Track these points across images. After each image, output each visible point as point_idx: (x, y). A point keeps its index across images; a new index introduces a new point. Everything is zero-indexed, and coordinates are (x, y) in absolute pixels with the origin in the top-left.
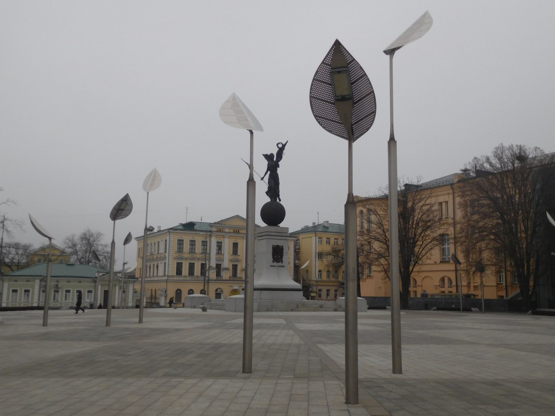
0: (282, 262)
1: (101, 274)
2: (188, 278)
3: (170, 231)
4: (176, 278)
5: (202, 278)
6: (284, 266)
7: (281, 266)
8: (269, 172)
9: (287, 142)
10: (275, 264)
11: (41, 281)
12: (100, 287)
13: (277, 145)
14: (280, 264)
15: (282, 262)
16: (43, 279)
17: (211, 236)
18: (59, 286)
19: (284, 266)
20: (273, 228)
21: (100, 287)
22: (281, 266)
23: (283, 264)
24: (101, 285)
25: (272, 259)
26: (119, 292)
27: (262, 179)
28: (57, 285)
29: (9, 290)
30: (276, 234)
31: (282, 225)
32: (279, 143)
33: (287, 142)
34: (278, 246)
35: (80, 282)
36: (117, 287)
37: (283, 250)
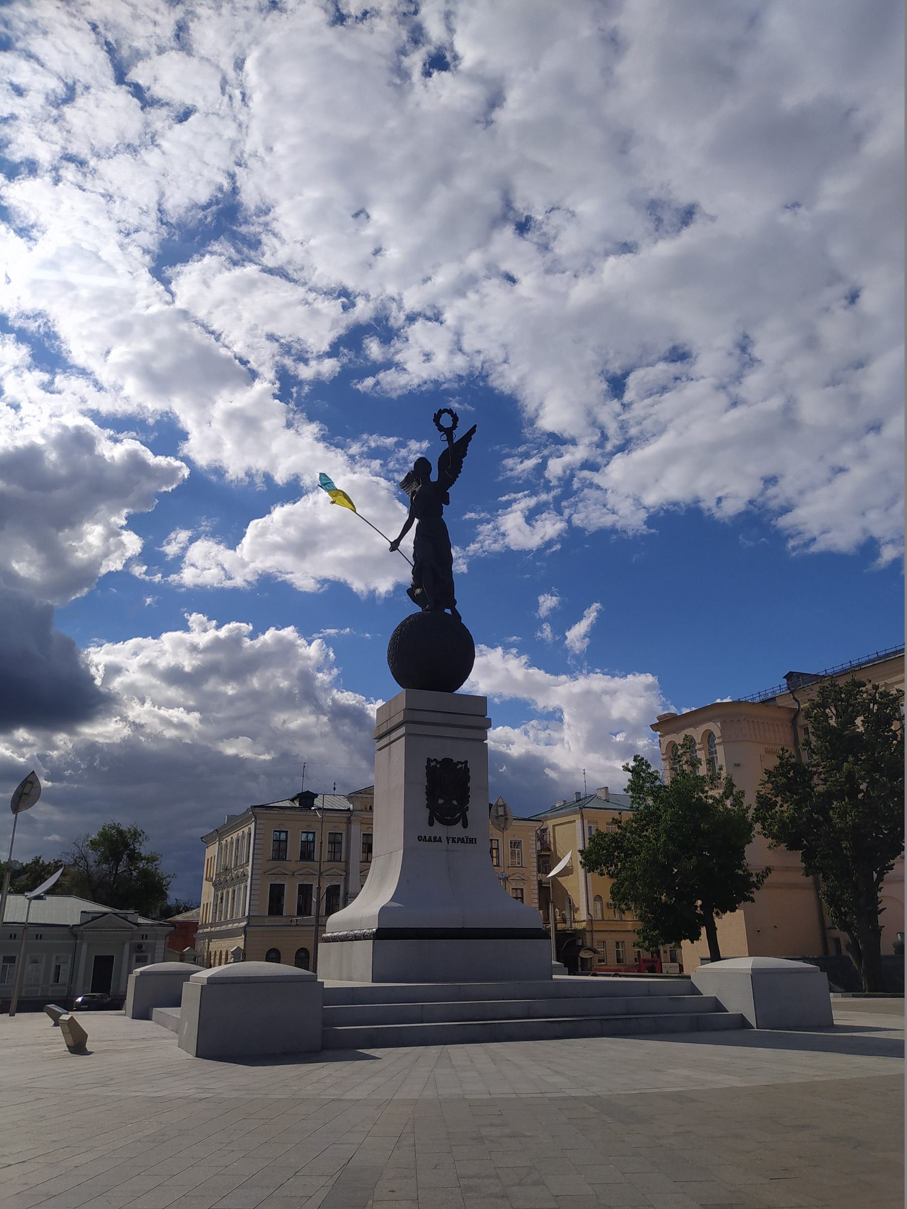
0: (465, 825)
3: (257, 810)
6: (472, 841)
7: (462, 840)
8: (416, 521)
10: (438, 829)
12: (84, 947)
13: (437, 419)
14: (457, 830)
15: (465, 825)
17: (349, 822)
19: (472, 841)
21: (84, 947)
22: (462, 840)
23: (469, 833)
25: (426, 812)
27: (395, 545)
30: (439, 718)
32: (441, 412)
33: (473, 430)
34: (447, 762)
37: (468, 779)
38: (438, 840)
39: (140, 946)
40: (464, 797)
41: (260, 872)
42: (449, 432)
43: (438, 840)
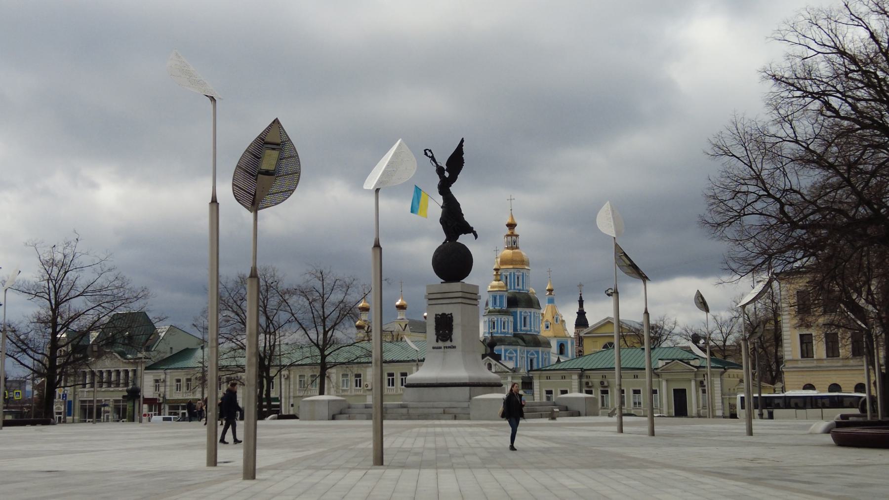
2: (825, 363)
4: (800, 365)
6: (454, 347)
9: (462, 141)
10: (441, 344)
11: (581, 377)
12: (664, 384)
13: (426, 154)
14: (448, 344)
16: (582, 373)
18: (606, 384)
19: (454, 347)
20: (455, 286)
23: (453, 344)
24: (667, 381)
25: (435, 337)
26: (697, 391)
30: (439, 296)
31: (466, 280)
33: (462, 141)
34: (444, 314)
35: (636, 377)
36: (693, 383)
37: (452, 321)
39: (702, 382)
40: (451, 329)
41: (788, 325)
42: (433, 158)
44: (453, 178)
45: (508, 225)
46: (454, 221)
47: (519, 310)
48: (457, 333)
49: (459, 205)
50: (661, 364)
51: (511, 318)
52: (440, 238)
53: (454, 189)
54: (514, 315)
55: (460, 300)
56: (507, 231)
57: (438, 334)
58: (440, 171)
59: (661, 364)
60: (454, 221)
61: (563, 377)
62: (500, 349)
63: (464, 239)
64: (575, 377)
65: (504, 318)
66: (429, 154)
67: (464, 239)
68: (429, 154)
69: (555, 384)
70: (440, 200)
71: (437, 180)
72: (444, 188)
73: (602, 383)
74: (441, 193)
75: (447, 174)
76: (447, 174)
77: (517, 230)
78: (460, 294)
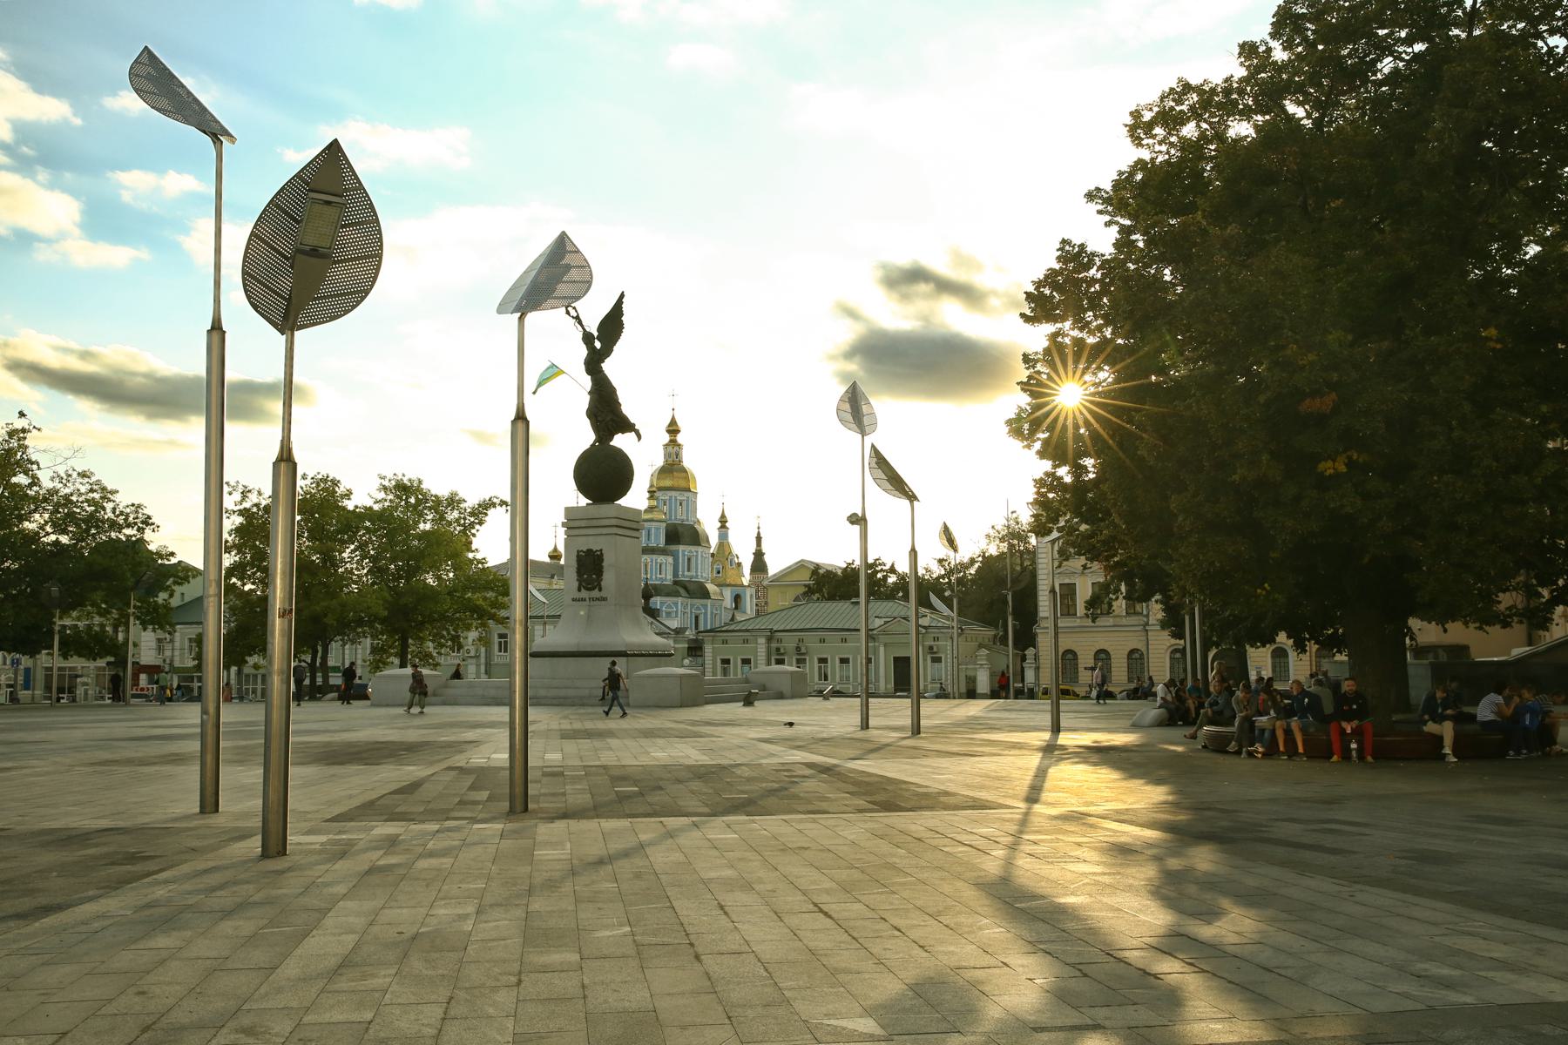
1: (882, 622)
5: (1133, 620)
6: (604, 599)
9: (622, 295)
10: (584, 594)
11: (769, 639)
12: (882, 649)
14: (595, 593)
19: (604, 599)
20: (605, 510)
23: (603, 594)
24: (885, 645)
25: (576, 584)
28: (798, 649)
29: (714, 661)
30: (583, 523)
31: (623, 502)
33: (622, 295)
34: (590, 551)
35: (844, 640)
38: (583, 600)
39: (931, 648)
40: (599, 572)
42: (577, 318)
43: (583, 600)
44: (607, 351)
45: (669, 431)
46: (606, 412)
47: (681, 548)
48: (608, 578)
49: (613, 390)
50: (878, 622)
51: (670, 559)
52: (585, 437)
53: (608, 367)
54: (675, 555)
55: (615, 530)
56: (667, 438)
57: (580, 580)
58: (588, 338)
59: (878, 622)
60: (606, 412)
61: (746, 641)
62: (656, 602)
63: (621, 441)
64: (762, 641)
65: (661, 559)
66: (573, 313)
67: (621, 441)
68: (573, 313)
69: (735, 652)
70: (587, 382)
71: (583, 352)
72: (594, 364)
73: (798, 649)
74: (589, 371)
75: (598, 345)
76: (598, 345)
77: (680, 438)
78: (614, 522)
